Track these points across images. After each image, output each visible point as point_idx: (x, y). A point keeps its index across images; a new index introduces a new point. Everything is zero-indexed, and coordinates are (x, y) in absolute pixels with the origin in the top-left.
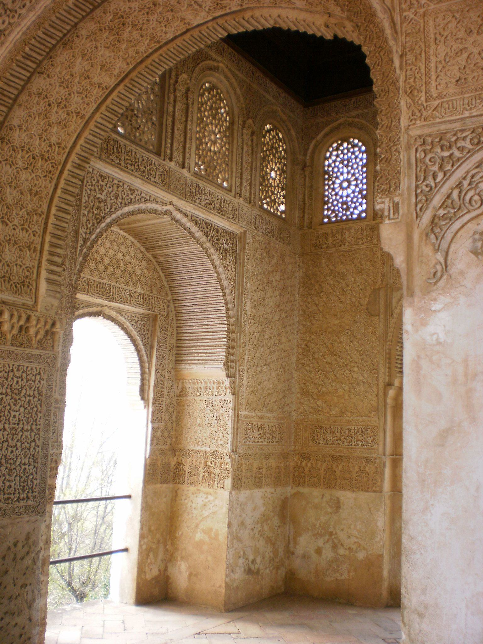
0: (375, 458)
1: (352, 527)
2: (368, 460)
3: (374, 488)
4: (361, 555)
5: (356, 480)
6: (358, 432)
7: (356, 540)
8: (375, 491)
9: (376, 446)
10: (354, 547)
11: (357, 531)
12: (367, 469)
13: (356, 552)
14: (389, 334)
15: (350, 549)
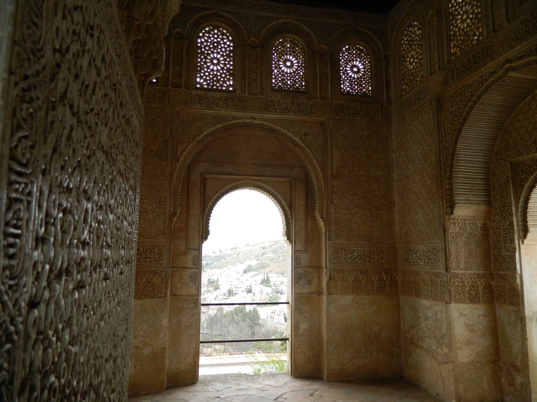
0: (162, 271)
1: (139, 328)
2: (155, 273)
3: (159, 295)
4: (147, 351)
5: (143, 290)
6: (146, 251)
7: (142, 339)
8: (160, 297)
9: (163, 261)
10: (141, 345)
11: (144, 331)
12: (154, 280)
13: (143, 349)
14: (175, 176)
15: (137, 348)
